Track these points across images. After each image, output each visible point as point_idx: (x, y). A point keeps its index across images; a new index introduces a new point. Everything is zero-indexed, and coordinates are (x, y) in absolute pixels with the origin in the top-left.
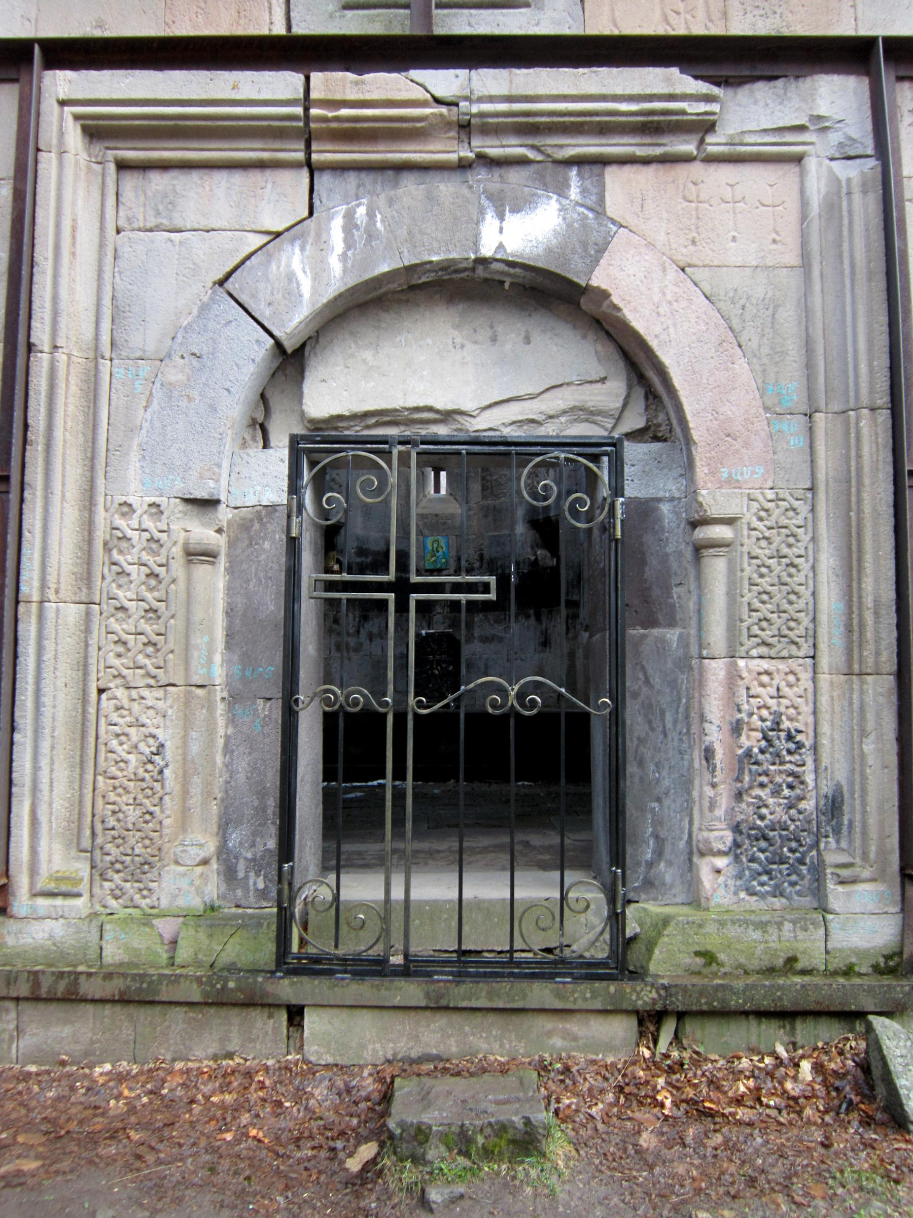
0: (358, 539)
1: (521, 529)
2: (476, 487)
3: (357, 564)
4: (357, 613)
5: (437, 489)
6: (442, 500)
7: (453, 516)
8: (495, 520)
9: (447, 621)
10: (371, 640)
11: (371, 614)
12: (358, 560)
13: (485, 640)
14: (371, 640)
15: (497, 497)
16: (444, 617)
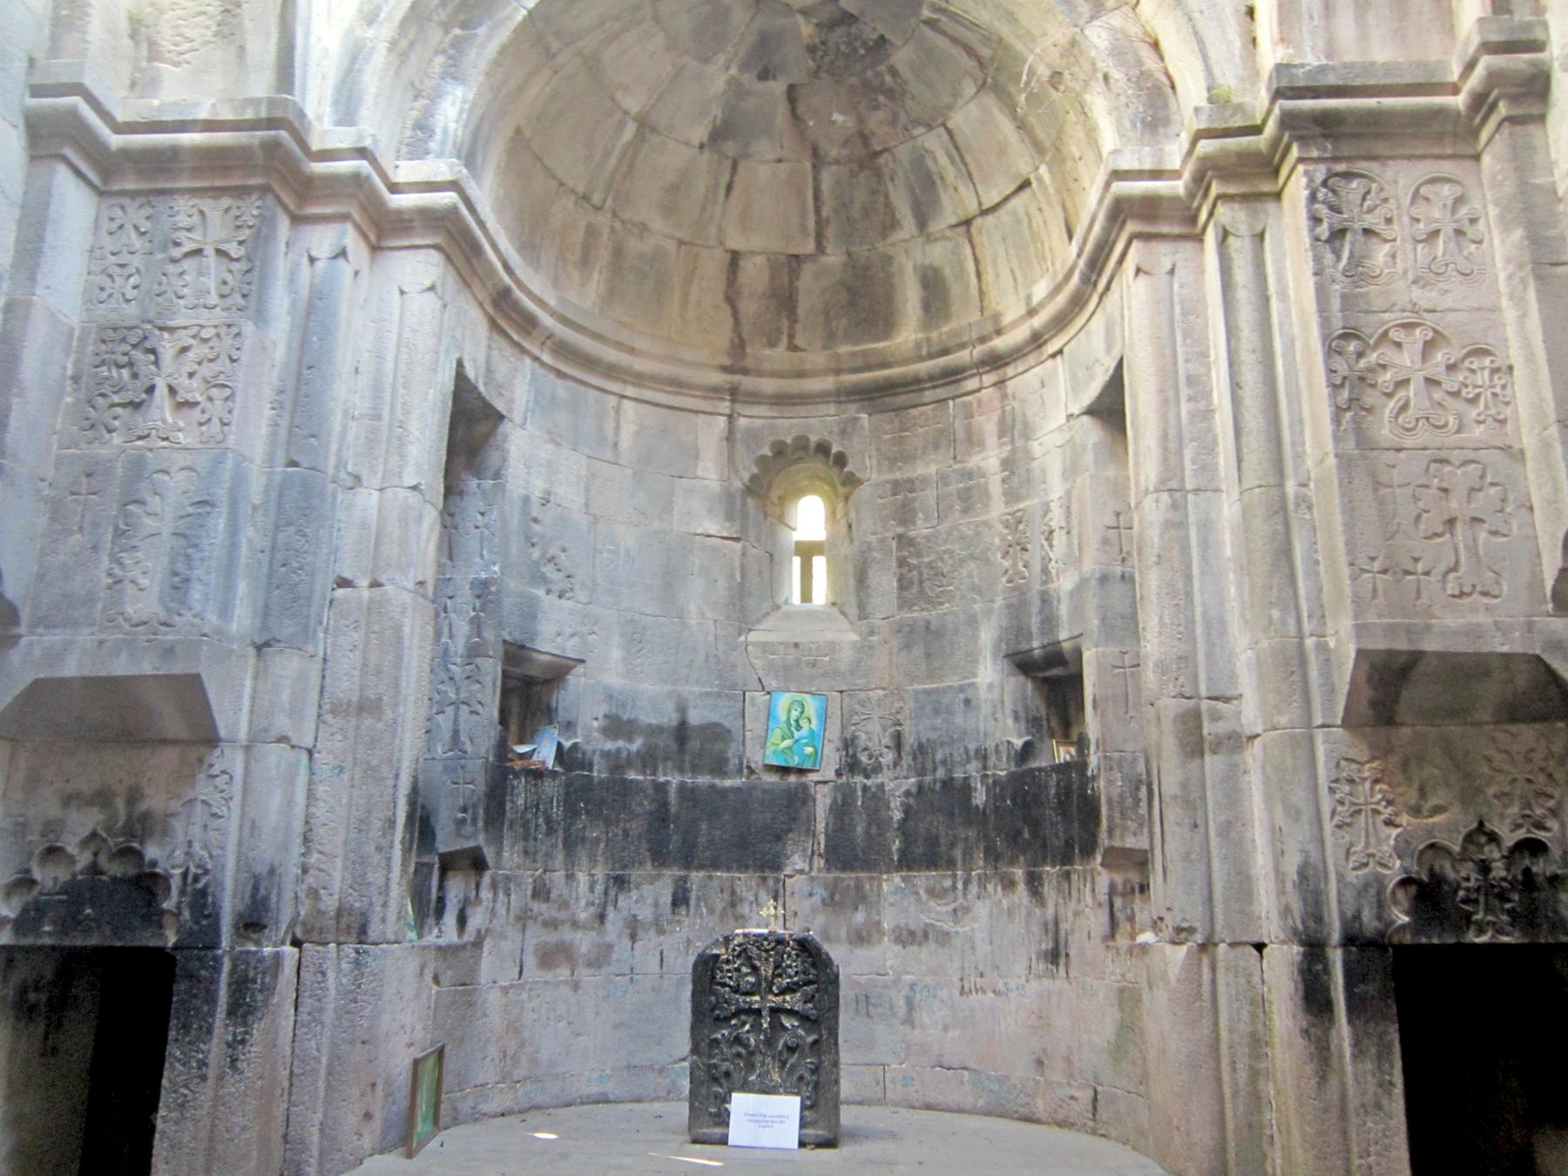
0: (610, 697)
1: (990, 676)
2: (884, 582)
3: (606, 755)
4: (600, 872)
5: (806, 596)
6: (813, 615)
7: (833, 647)
8: (928, 655)
9: (820, 892)
10: (633, 937)
11: (635, 874)
12: (609, 746)
13: (906, 937)
14: (633, 937)
15: (933, 602)
16: (812, 879)
